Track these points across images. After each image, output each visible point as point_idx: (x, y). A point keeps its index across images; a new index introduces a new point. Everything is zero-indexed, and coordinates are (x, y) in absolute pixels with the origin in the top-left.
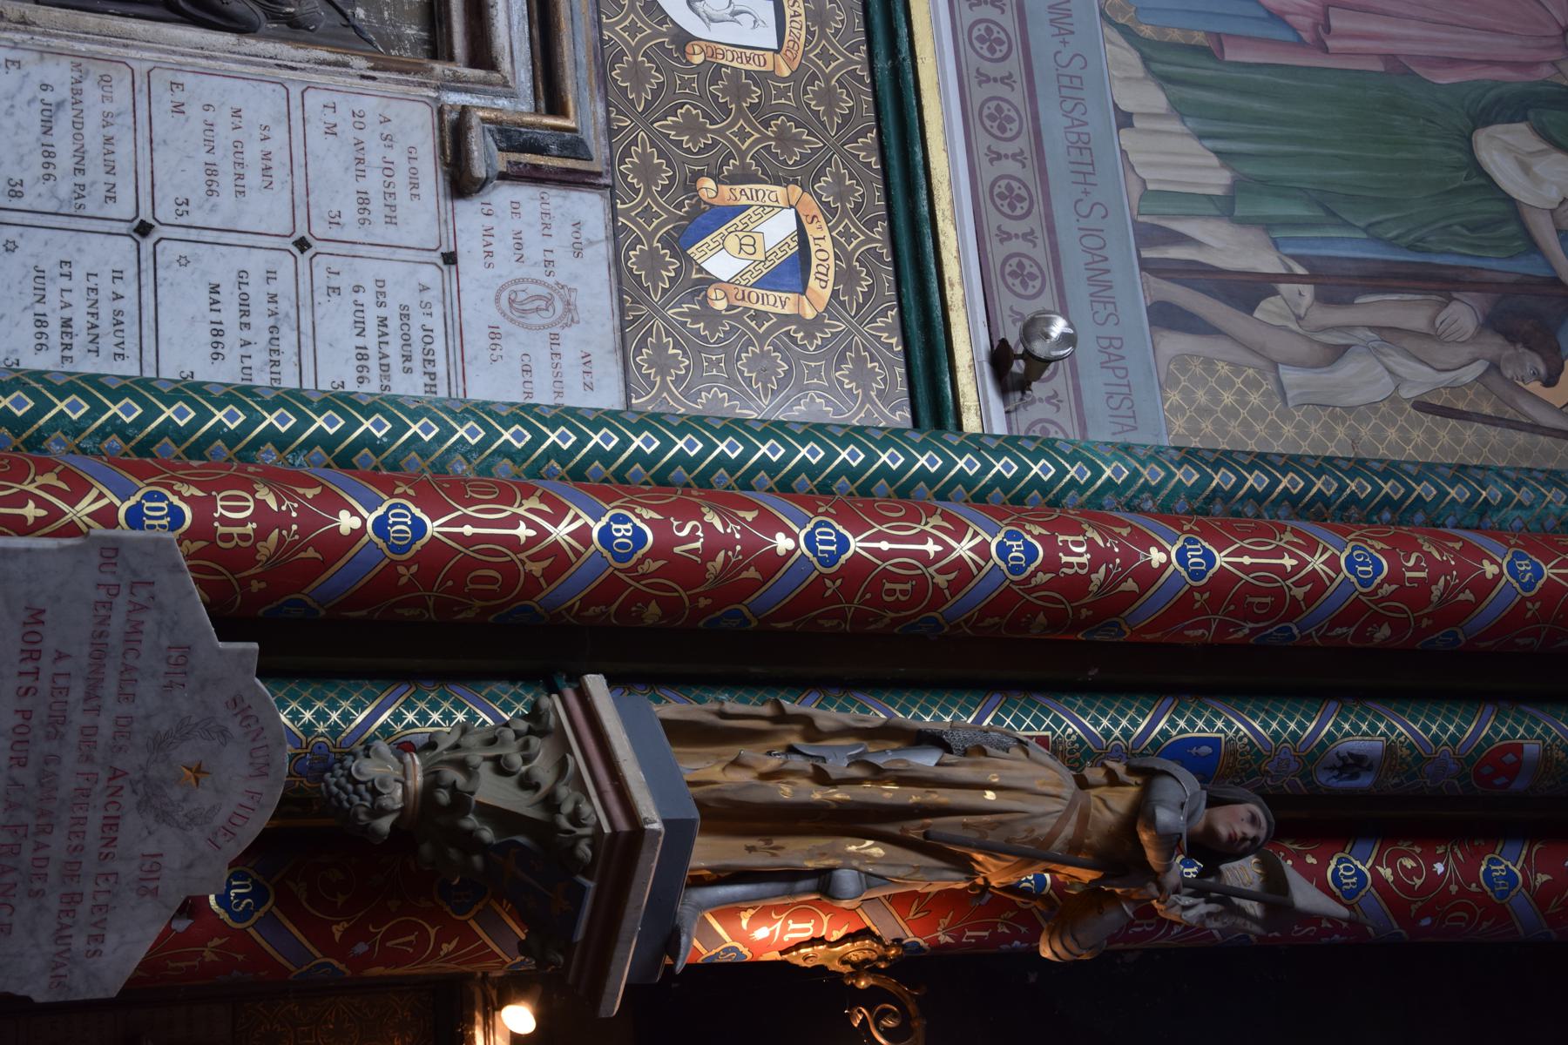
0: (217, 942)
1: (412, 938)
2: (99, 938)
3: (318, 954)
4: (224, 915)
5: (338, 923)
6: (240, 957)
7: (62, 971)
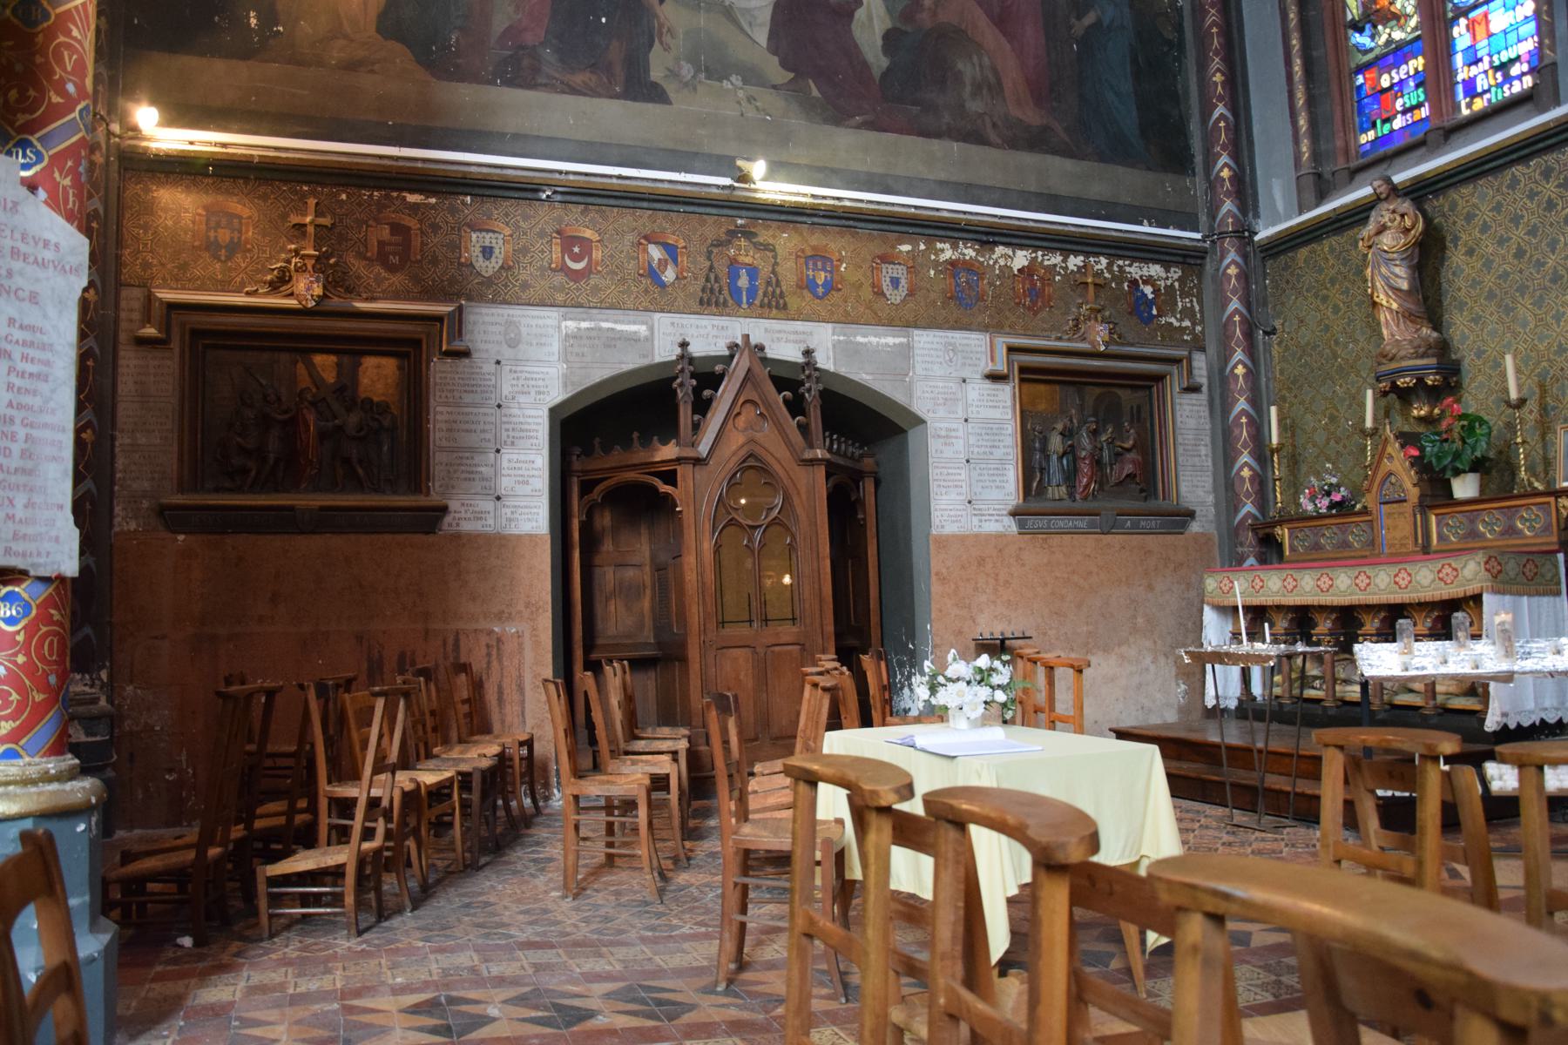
0: (57, 175)
1: (66, 53)
2: (46, 244)
3: (72, 116)
4: (38, 168)
5: (50, 98)
6: (70, 163)
7: (68, 268)
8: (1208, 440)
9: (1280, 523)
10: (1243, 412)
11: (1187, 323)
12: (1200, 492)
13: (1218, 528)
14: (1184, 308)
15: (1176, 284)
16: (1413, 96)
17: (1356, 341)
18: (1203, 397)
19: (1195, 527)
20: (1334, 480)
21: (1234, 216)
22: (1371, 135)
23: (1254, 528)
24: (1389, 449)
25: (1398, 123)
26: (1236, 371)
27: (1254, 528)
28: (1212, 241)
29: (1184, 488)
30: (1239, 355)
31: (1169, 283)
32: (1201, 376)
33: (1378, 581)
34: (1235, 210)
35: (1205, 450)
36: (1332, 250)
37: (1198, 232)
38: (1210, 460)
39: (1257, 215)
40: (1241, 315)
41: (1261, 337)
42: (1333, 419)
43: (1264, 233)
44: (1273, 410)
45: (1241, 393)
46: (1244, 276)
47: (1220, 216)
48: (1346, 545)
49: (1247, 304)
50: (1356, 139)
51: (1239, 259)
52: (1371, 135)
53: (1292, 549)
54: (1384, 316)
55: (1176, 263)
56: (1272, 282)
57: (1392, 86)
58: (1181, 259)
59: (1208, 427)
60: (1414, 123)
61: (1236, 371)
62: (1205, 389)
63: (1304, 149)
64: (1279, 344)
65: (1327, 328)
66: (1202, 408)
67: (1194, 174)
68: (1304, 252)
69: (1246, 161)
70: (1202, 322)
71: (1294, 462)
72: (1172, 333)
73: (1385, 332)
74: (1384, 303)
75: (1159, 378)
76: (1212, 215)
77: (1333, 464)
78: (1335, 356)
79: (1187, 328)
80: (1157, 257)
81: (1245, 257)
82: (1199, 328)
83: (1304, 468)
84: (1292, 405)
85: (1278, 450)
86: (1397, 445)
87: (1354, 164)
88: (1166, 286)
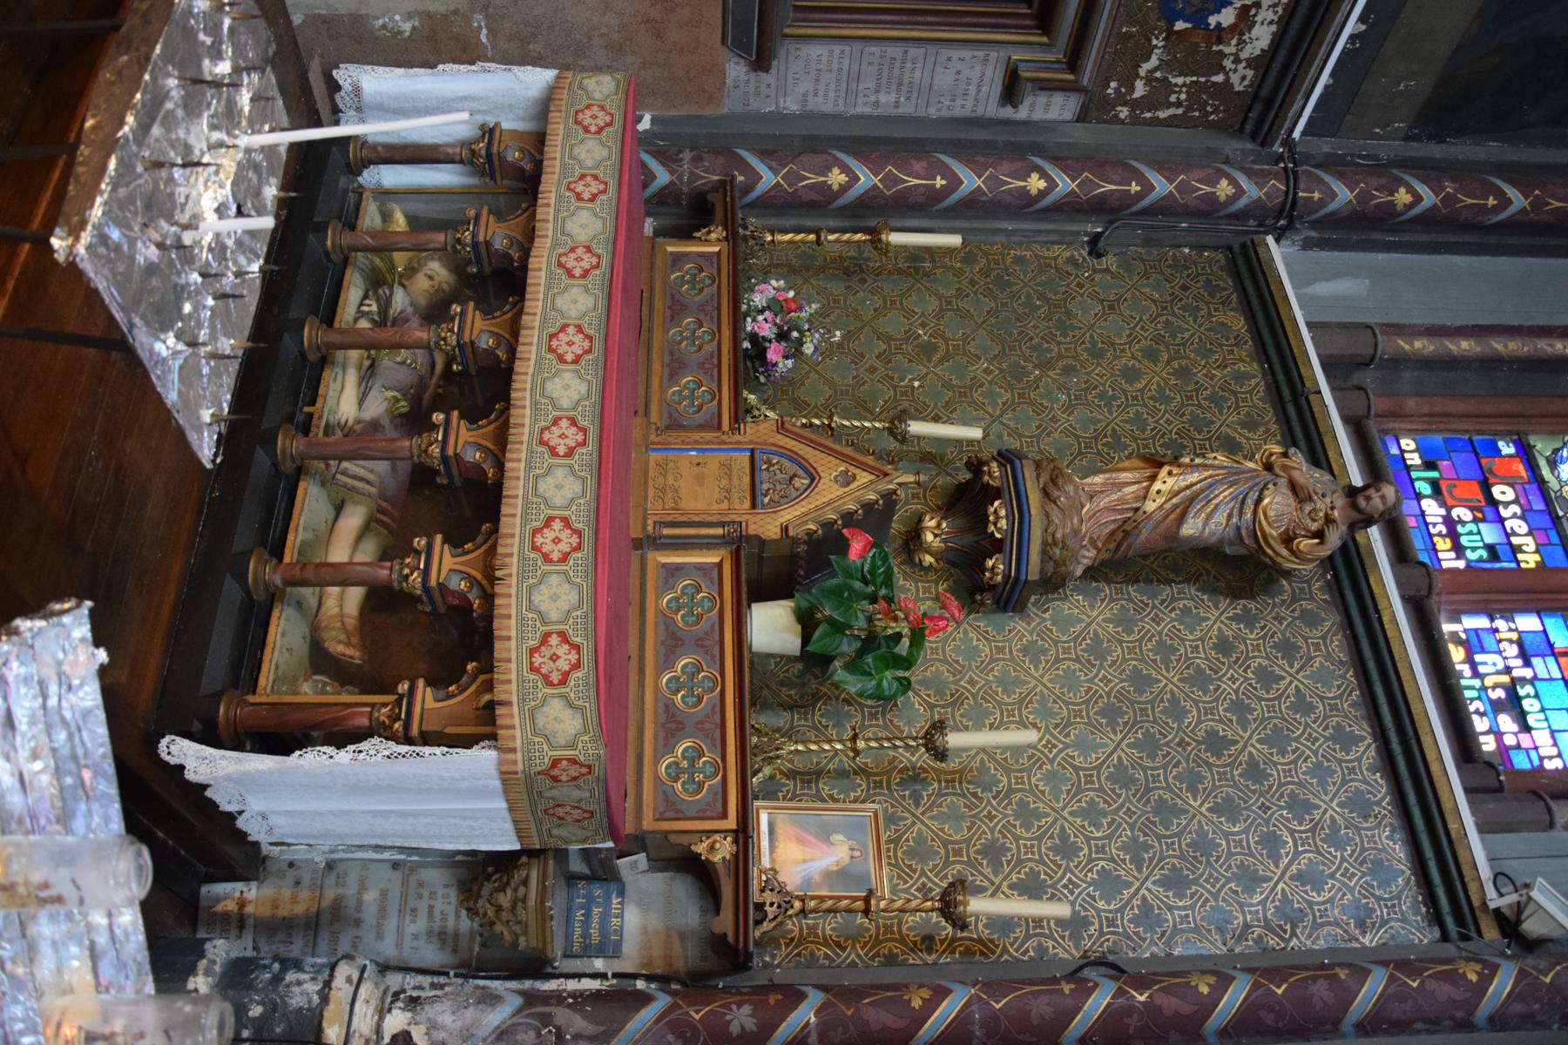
8: (907, 109)
9: (732, 238)
10: (955, 182)
11: (1140, 89)
12: (805, 86)
13: (734, 117)
14: (1169, 87)
15: (1219, 78)
16: (1479, 537)
17: (1069, 408)
18: (992, 108)
19: (736, 70)
20: (808, 349)
21: (1322, 203)
22: (1414, 459)
23: (725, 186)
24: (864, 478)
25: (1432, 508)
26: (1035, 176)
27: (725, 186)
28: (1280, 158)
29: (816, 51)
30: (1065, 184)
31: (1228, 64)
32: (1047, 106)
33: (560, 473)
34: (1333, 206)
35: (887, 101)
36: (1240, 377)
37: (1304, 133)
38: (867, 110)
39: (1308, 245)
40: (1140, 196)
41: (1089, 228)
42: (927, 350)
43: (1278, 252)
44: (955, 240)
45: (993, 181)
46: (1209, 210)
47: (1327, 178)
48: (676, 367)
49: (1164, 209)
50: (1410, 433)
51: (1243, 202)
52: (1414, 459)
53: (678, 259)
54: (1129, 478)
55: (1259, 84)
56: (1186, 258)
57: (1494, 503)
58: (1264, 93)
59: (933, 112)
60: (1431, 536)
61: (1035, 176)
62: (1008, 112)
63: (1418, 344)
64: (1072, 261)
65: (1097, 355)
66: (969, 105)
67: (1407, 139)
68: (1238, 324)
69: (1406, 237)
70: (1135, 120)
71: (851, 270)
72: (1130, 53)
73: (1098, 479)
74: (1157, 486)
75: (1045, 21)
76: (1331, 163)
77: (840, 345)
78: (1045, 365)
79: (1132, 88)
80: (1287, 44)
81: (1240, 216)
82: (1124, 112)
83: (836, 288)
84: (958, 274)
85: (876, 242)
86: (872, 497)
87: (1372, 425)
88: (1222, 55)
